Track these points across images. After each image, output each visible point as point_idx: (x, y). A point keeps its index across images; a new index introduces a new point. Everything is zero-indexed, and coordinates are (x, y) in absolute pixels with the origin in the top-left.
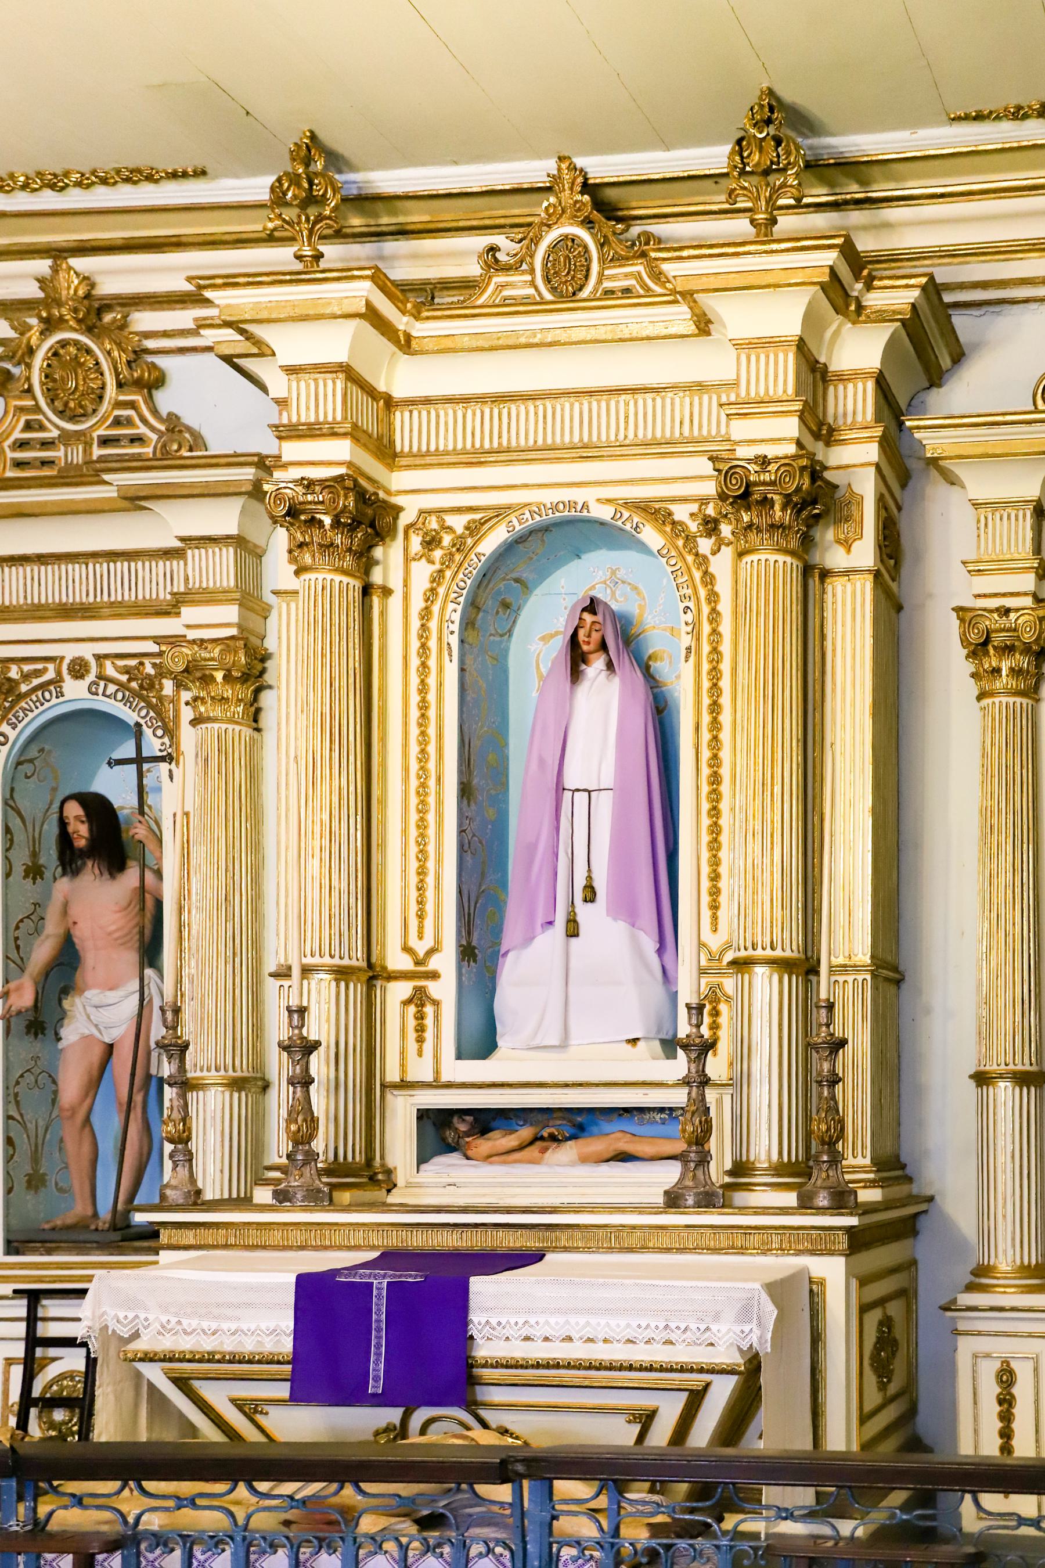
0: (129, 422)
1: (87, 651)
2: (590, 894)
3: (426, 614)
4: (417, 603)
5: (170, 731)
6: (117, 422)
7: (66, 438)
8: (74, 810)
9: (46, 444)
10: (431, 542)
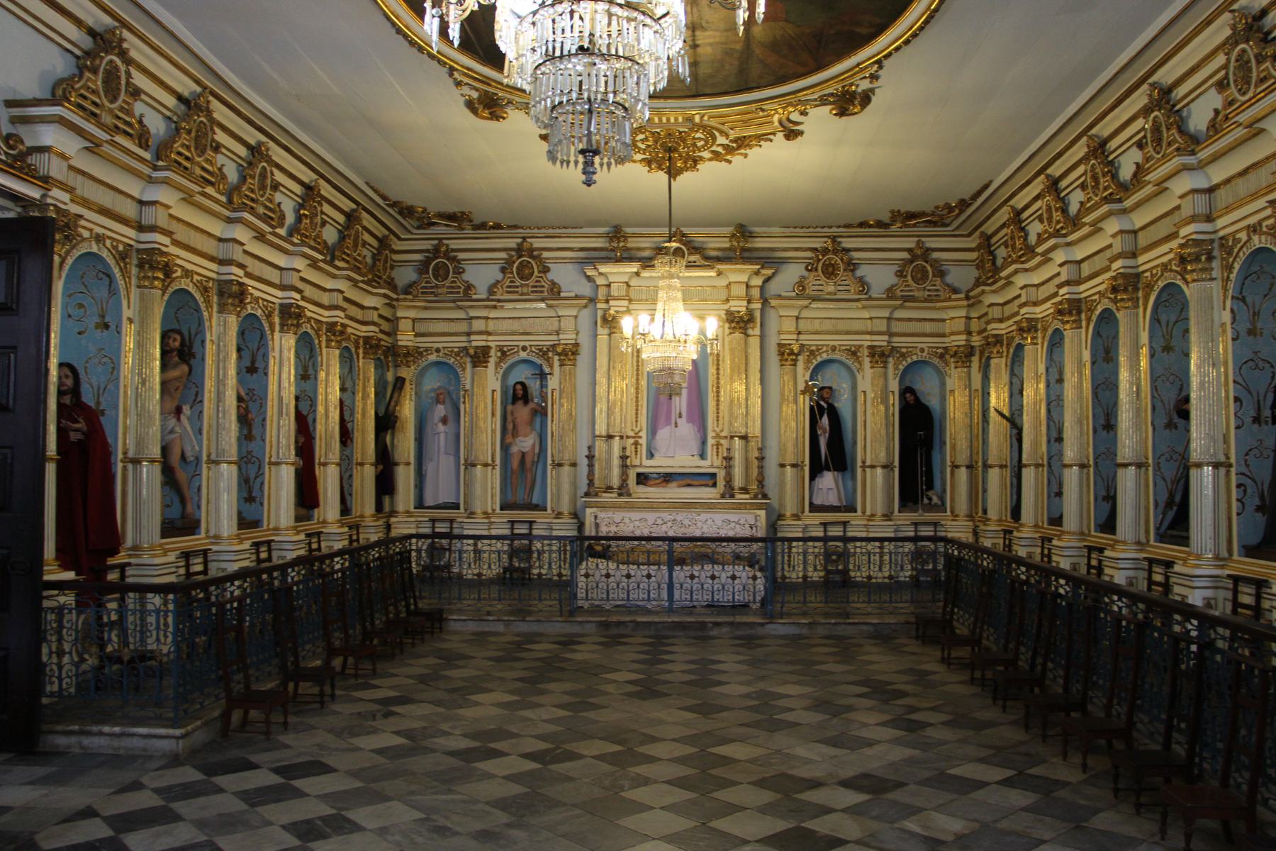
1: (527, 344)
2: (680, 416)
5: (551, 366)
6: (537, 281)
7: (522, 286)
8: (519, 387)
9: (517, 287)
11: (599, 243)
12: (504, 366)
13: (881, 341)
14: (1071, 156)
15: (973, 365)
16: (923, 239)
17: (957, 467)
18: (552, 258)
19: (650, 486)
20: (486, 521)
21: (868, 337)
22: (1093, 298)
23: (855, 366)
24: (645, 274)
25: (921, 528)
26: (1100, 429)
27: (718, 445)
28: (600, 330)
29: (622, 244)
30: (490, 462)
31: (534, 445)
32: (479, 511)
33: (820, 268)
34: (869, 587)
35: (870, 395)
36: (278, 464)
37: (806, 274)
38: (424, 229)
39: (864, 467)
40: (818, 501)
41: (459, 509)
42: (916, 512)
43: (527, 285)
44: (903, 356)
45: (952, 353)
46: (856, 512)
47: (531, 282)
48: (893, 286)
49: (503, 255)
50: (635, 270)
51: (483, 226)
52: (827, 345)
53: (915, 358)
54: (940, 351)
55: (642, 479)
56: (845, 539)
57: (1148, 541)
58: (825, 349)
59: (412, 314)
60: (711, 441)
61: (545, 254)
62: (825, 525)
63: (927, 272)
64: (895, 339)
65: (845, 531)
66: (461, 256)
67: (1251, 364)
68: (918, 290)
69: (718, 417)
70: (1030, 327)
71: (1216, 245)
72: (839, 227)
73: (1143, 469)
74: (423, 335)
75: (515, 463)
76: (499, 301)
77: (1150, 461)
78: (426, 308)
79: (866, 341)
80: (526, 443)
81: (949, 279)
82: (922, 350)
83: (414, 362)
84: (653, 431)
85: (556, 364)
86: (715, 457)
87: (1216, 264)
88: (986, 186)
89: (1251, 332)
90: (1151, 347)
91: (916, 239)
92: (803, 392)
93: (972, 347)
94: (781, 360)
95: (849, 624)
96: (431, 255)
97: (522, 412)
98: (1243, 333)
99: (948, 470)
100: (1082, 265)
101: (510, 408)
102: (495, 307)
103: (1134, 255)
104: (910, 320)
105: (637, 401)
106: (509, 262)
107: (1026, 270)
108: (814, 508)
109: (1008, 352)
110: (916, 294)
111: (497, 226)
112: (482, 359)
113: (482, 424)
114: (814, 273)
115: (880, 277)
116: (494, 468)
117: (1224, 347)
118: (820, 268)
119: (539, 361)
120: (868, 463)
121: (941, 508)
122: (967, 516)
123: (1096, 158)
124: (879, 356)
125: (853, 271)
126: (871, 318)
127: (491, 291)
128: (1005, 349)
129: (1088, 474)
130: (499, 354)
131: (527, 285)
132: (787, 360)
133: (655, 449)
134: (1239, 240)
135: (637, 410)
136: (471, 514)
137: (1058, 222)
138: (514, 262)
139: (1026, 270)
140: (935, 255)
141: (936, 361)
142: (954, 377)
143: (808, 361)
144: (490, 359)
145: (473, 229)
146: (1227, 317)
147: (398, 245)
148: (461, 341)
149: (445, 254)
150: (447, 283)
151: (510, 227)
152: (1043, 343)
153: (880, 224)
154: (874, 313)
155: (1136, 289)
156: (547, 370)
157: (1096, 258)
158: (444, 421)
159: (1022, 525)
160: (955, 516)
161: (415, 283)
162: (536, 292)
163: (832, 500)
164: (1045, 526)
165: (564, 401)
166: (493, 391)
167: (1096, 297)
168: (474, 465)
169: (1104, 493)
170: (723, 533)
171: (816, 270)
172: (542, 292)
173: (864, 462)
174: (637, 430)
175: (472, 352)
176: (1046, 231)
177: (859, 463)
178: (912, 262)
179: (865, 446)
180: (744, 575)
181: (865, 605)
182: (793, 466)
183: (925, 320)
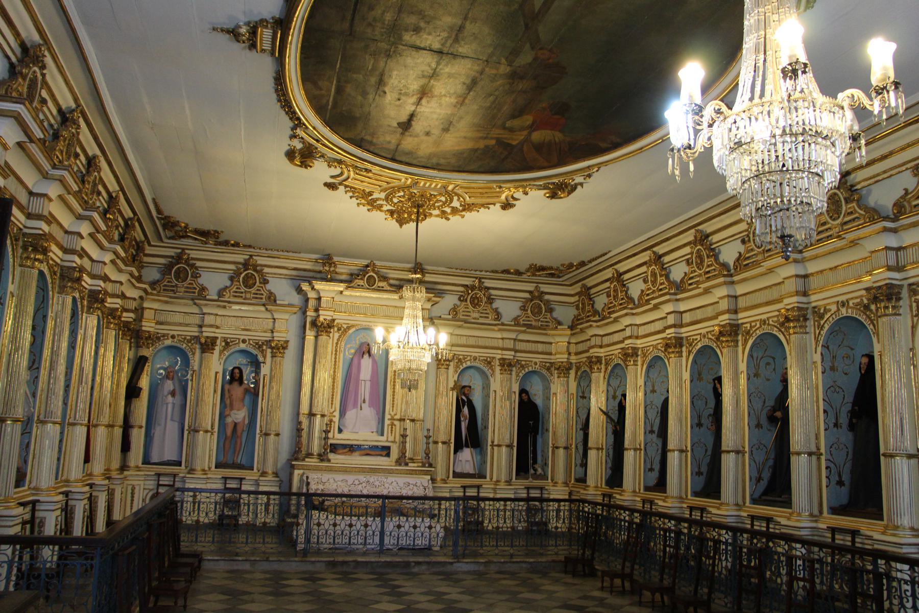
0: (260, 290)
1: (246, 338)
2: (364, 401)
3: (337, 344)
4: (335, 341)
5: (265, 357)
6: (258, 290)
7: (245, 292)
8: (237, 371)
9: (242, 293)
10: (339, 329)
11: (308, 266)
12: (227, 354)
13: (509, 355)
14: (676, 241)
16: (540, 285)
17: (557, 448)
18: (272, 274)
19: (339, 454)
20: (205, 476)
21: (499, 352)
22: (694, 337)
23: (489, 372)
24: (346, 293)
25: (531, 491)
26: (695, 426)
27: (392, 424)
28: (308, 332)
29: (332, 269)
30: (209, 429)
31: (244, 417)
32: (199, 468)
33: (469, 300)
34: (497, 534)
35: (500, 393)
36: (74, 424)
37: (458, 303)
38: (176, 239)
39: (492, 445)
40: (458, 470)
41: (180, 466)
42: (527, 479)
43: (250, 292)
44: (523, 367)
45: (557, 367)
46: (485, 478)
47: (253, 290)
48: (519, 316)
49: (233, 267)
50: (341, 289)
51: (226, 243)
52: (471, 356)
53: (530, 369)
54: (548, 365)
55: (334, 448)
56: (478, 499)
57: (744, 503)
58: (469, 358)
59: (156, 306)
60: (387, 422)
61: (266, 270)
62: (464, 487)
63: (541, 308)
64: (518, 354)
65: (478, 492)
66: (198, 264)
67: (832, 389)
69: (393, 404)
70: (630, 354)
71: (810, 311)
72: (486, 271)
73: (740, 455)
74: (162, 323)
75: (229, 431)
76: (229, 302)
77: (747, 449)
78: (167, 302)
79: (498, 354)
80: (239, 415)
81: (555, 314)
82: (536, 364)
83: (153, 345)
84: (343, 413)
85: (269, 355)
86: (390, 434)
87: (810, 323)
88: (606, 254)
89: (832, 369)
90: (748, 374)
91: (535, 285)
92: (453, 389)
93: (571, 363)
94: (438, 365)
95: (514, 562)
96: (174, 261)
97: (237, 391)
98: (828, 368)
100: (684, 315)
101: (227, 387)
102: (225, 307)
103: (736, 312)
104: (528, 341)
105: (333, 389)
106: (237, 273)
107: (633, 314)
108: (456, 475)
109: (606, 369)
110: (533, 323)
111: (237, 245)
112: (210, 346)
113: (206, 398)
114: (464, 303)
115: (509, 309)
116: (212, 434)
117: (817, 377)
118: (469, 300)
119: (255, 352)
120: (496, 443)
121: (544, 477)
123: (702, 245)
124: (506, 365)
125: (491, 303)
126: (502, 339)
127: (221, 293)
128: (603, 366)
129: (686, 456)
130: (223, 344)
131: (250, 292)
132: (443, 365)
133: (344, 426)
134: (830, 310)
135: (333, 395)
136: (192, 471)
137: (661, 284)
138: (241, 273)
139: (633, 314)
140: (547, 297)
141: (544, 372)
143: (457, 367)
144: (216, 348)
145: (215, 245)
147: (149, 250)
148: (193, 331)
149: (186, 261)
150: (185, 284)
151: (245, 246)
152: (642, 365)
153: (518, 273)
154: (505, 335)
155: (737, 334)
156: (261, 359)
157: (698, 311)
158: (173, 394)
159: (623, 491)
160: (555, 484)
161: (158, 281)
162: (256, 298)
163: (469, 468)
164: (642, 491)
165: (274, 384)
166: (217, 373)
167: (698, 337)
168: (197, 431)
169: (697, 470)
170: (404, 492)
171: (466, 301)
172: (262, 298)
173: (493, 442)
174: (332, 411)
175: (203, 340)
176: (648, 289)
177: (489, 443)
178: (532, 300)
179: (494, 430)
180: (407, 525)
181: (509, 548)
182: (444, 443)
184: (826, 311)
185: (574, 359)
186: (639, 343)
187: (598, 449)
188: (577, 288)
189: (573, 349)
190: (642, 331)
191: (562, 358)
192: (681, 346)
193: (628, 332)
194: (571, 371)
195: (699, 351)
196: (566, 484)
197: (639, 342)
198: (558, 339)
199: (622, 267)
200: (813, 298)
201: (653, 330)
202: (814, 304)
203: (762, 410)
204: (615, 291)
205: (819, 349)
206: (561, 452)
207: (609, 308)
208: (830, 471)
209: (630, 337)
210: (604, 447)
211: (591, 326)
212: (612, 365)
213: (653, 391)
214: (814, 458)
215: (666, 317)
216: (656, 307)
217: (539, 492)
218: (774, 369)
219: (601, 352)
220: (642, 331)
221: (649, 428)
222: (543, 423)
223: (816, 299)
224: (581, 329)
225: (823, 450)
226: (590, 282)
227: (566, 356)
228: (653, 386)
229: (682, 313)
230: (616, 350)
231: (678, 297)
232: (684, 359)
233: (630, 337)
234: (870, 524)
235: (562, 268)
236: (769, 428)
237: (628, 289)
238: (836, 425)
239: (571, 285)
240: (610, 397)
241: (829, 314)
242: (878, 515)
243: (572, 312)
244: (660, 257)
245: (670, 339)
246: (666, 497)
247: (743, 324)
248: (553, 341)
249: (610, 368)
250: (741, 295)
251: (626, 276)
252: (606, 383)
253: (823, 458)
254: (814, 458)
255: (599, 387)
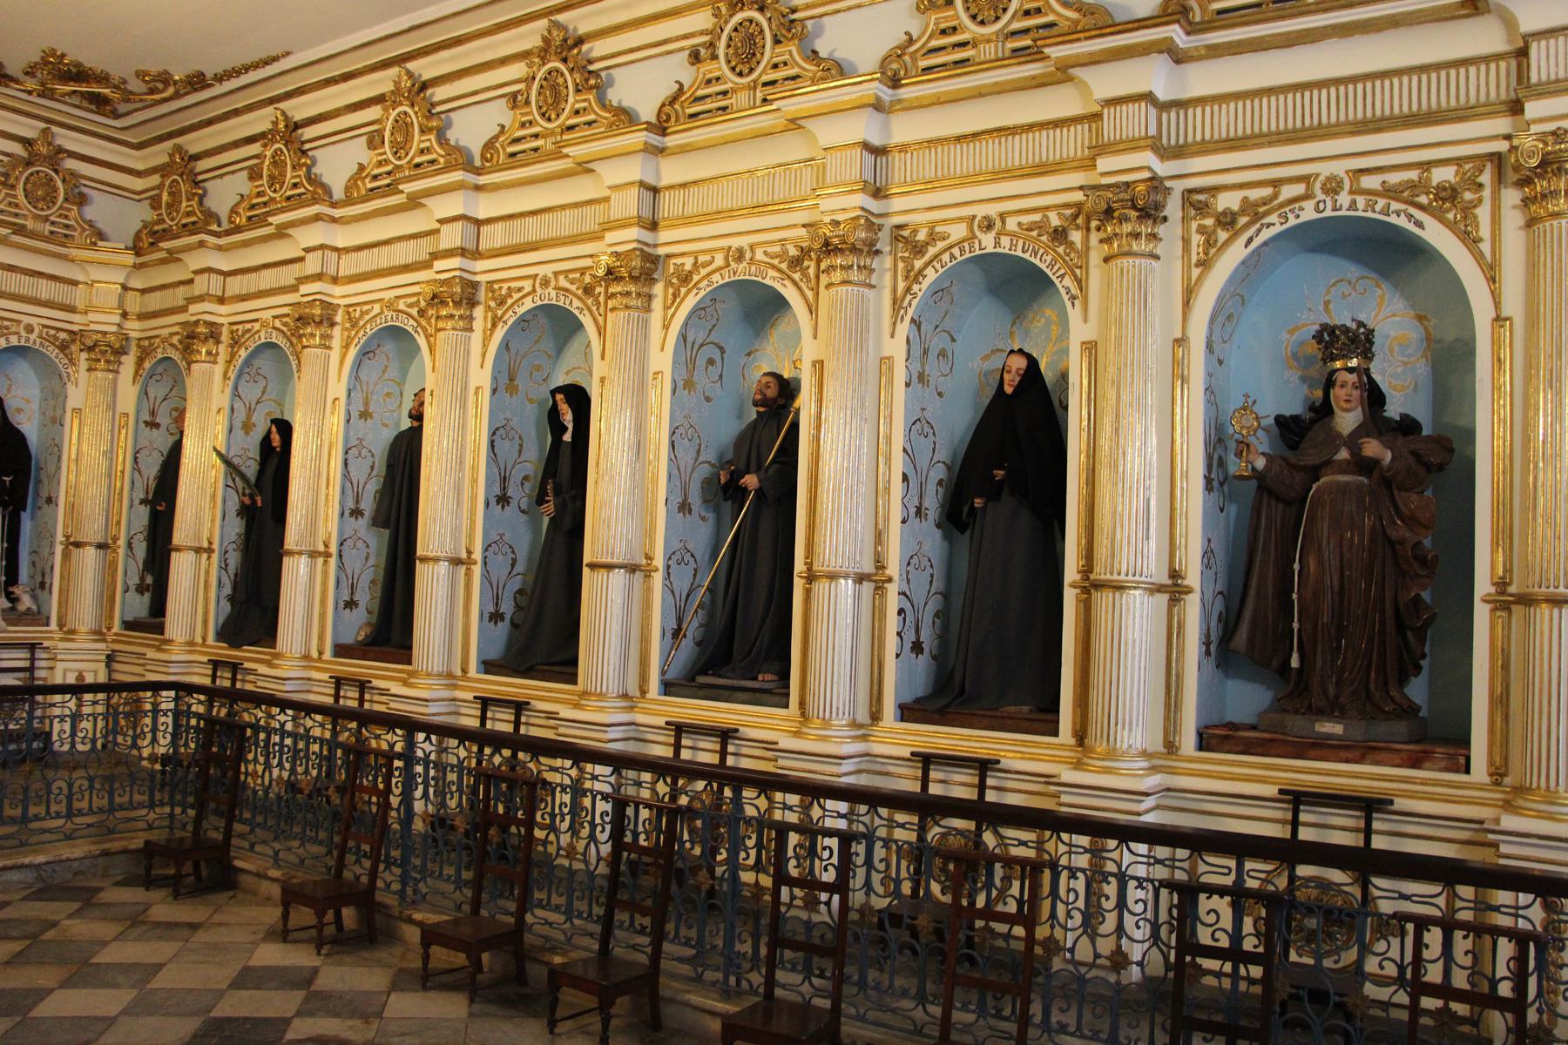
15: (122, 369)
16: (55, 129)
17: (78, 545)
22: (514, 285)
26: (493, 502)
45: (89, 343)
53: (14, 341)
54: (63, 335)
57: (643, 692)
63: (55, 190)
68: (36, 217)
81: (90, 212)
82: (29, 329)
88: (275, 59)
91: (43, 125)
99: (59, 549)
100: (485, 229)
103: (653, 226)
107: (334, 220)
109: (233, 356)
110: (30, 224)
121: (38, 617)
122: (95, 632)
123: (565, 60)
129: (468, 574)
139: (334, 220)
140: (71, 164)
141: (53, 352)
142: (82, 386)
146: (896, 348)
152: (346, 347)
157: (530, 220)
159: (278, 656)
160: (69, 634)
164: (328, 655)
169: (492, 609)
178: (29, 164)
183: (40, 274)
184: (933, 238)
185: (134, 328)
186: (339, 294)
187: (198, 550)
188: (159, 155)
189: (134, 303)
190: (348, 265)
191: (105, 322)
192: (473, 303)
193: (312, 265)
194: (124, 359)
195: (523, 321)
196: (99, 634)
197: (338, 290)
198: (95, 273)
199: (300, 109)
200: (897, 204)
201: (384, 264)
202: (897, 220)
203: (694, 469)
204: (277, 163)
205: (904, 328)
206: (89, 558)
207: (253, 207)
208: (904, 619)
209: (319, 277)
210: (216, 546)
211: (202, 244)
212: (252, 346)
213: (365, 415)
214: (867, 587)
215: (437, 231)
216: (414, 202)
217: (25, 654)
218: (721, 376)
219: (222, 314)
220: (348, 265)
221: (351, 504)
222: (39, 482)
223: (905, 207)
224: (169, 251)
225: (894, 568)
226: (195, 142)
227: (117, 319)
228: (366, 404)
229: (479, 223)
230: (269, 310)
231: (483, 180)
232: (477, 337)
233: (319, 277)
234: (1024, 743)
235: (136, 86)
236: (703, 514)
237: (314, 162)
238: (919, 511)
239: (140, 146)
240: (238, 424)
241: (941, 245)
242: (1044, 717)
243: (140, 214)
244: (424, 86)
245: (444, 282)
246: (413, 674)
247: (669, 256)
248: (80, 278)
249: (243, 353)
250: (672, 187)
251: (309, 132)
252: (228, 391)
253: (892, 590)
254: (867, 587)
255: (209, 398)
